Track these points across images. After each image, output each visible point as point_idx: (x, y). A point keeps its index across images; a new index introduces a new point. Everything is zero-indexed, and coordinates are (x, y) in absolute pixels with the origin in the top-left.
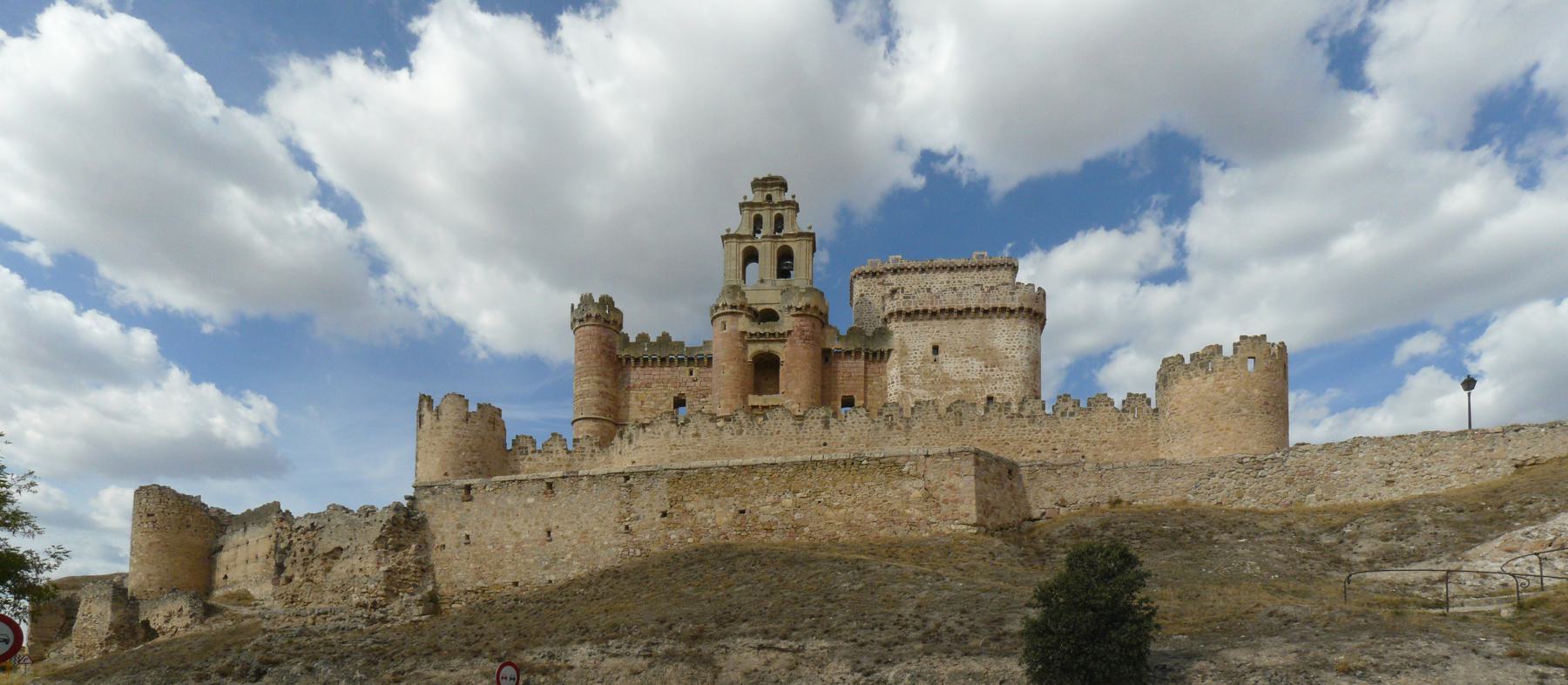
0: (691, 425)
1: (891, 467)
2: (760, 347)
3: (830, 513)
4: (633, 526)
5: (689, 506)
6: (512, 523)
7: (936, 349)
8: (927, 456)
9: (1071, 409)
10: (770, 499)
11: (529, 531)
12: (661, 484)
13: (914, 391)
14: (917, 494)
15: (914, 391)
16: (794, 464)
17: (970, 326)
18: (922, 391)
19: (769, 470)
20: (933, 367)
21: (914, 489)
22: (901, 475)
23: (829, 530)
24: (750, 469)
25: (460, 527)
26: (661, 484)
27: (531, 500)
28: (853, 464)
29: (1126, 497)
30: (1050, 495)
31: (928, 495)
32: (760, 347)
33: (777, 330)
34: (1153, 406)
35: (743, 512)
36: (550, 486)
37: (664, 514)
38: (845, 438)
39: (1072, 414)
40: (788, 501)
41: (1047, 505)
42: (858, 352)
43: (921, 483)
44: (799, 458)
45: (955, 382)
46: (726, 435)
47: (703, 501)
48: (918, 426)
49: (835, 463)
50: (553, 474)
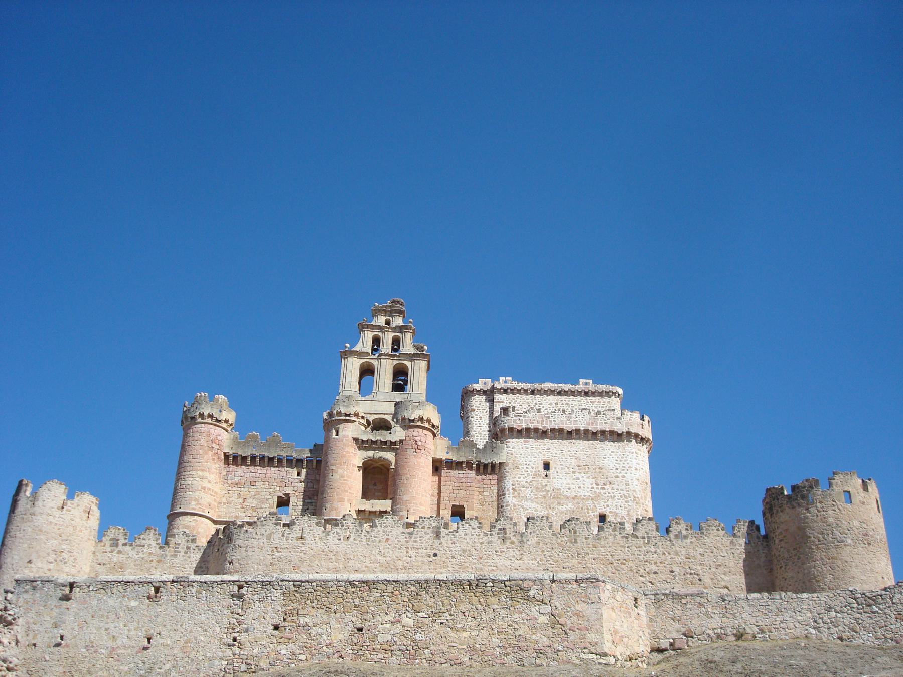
0: (296, 528)
1: (516, 590)
3: (452, 634)
4: (242, 638)
5: (303, 621)
6: (112, 626)
7: (547, 466)
8: (553, 581)
9: (684, 532)
10: (391, 617)
12: (277, 594)
13: (527, 504)
15: (527, 504)
16: (418, 582)
17: (581, 445)
18: (534, 505)
19: (390, 587)
20: (545, 482)
21: (540, 615)
22: (528, 599)
23: (454, 654)
24: (370, 584)
25: (56, 626)
26: (277, 594)
27: (134, 603)
29: (751, 630)
30: (677, 625)
31: (555, 621)
32: (371, 453)
34: (763, 532)
35: (360, 630)
36: (157, 590)
37: (276, 628)
39: (686, 537)
41: (675, 635)
43: (546, 609)
44: (420, 576)
45: (567, 498)
46: (332, 539)
47: (320, 615)
48: (533, 540)
49: (459, 583)
50: (164, 578)
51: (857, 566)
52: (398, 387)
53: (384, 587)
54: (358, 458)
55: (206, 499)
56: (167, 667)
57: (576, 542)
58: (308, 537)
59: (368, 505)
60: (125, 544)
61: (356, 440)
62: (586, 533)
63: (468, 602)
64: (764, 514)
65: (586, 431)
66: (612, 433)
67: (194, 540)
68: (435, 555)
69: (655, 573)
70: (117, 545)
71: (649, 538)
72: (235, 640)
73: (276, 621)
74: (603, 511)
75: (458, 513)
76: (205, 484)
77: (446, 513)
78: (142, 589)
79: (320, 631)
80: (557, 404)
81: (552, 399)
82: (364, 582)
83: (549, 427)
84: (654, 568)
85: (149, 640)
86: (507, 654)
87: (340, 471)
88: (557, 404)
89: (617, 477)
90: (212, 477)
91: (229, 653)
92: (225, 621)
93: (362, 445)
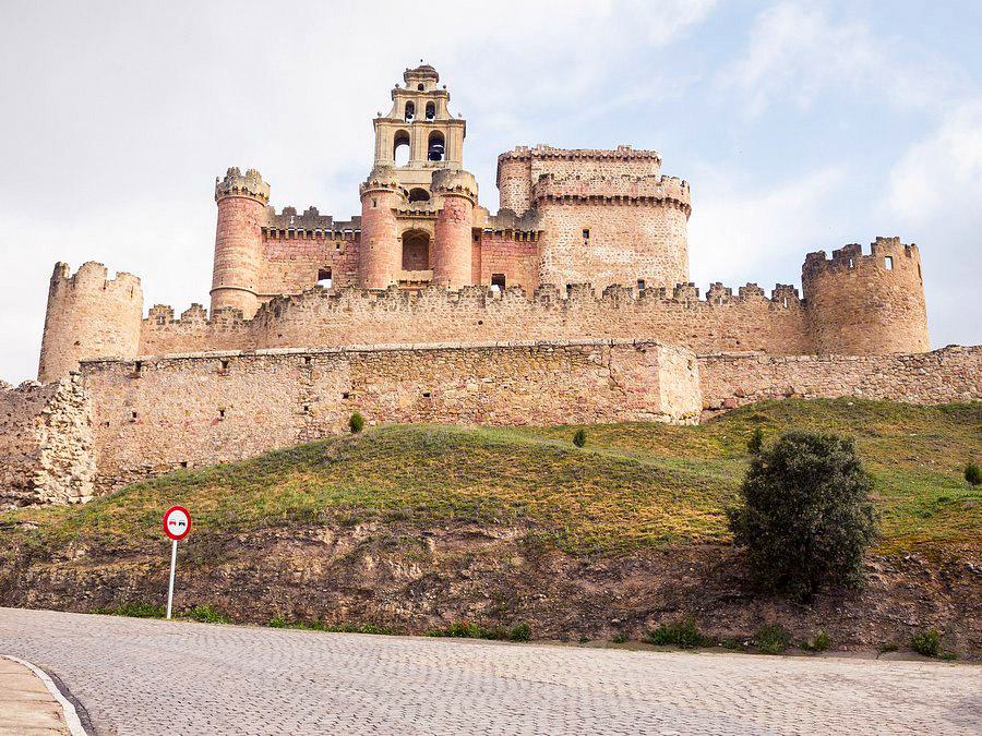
1: (576, 354)
2: (409, 224)
4: (313, 406)
5: (371, 388)
7: (586, 233)
9: (724, 297)
11: (200, 408)
13: (566, 272)
14: (602, 382)
15: (566, 272)
16: (480, 349)
19: (454, 355)
20: (584, 249)
23: (518, 415)
27: (203, 379)
28: (538, 350)
30: (728, 386)
31: (614, 384)
32: (409, 224)
33: (427, 209)
34: (801, 297)
35: (427, 395)
36: (225, 364)
38: (501, 317)
39: (725, 302)
40: (473, 386)
41: (726, 395)
42: (508, 232)
46: (379, 311)
47: (387, 384)
48: (576, 307)
50: (231, 353)
51: (894, 330)
52: (435, 156)
53: (448, 355)
54: (397, 229)
55: (248, 274)
56: (243, 436)
57: (618, 307)
58: (356, 309)
59: (409, 276)
60: (172, 322)
61: (394, 210)
62: (628, 299)
63: (534, 367)
64: (803, 279)
65: (626, 198)
66: (651, 199)
67: (240, 315)
68: (481, 323)
70: (164, 323)
71: (689, 303)
72: (306, 408)
73: (345, 390)
74: (641, 277)
75: (499, 280)
76: (245, 259)
77: (487, 281)
78: (211, 366)
79: (388, 398)
80: (595, 170)
81: (590, 165)
82: (428, 350)
83: (589, 194)
84: (693, 332)
85: (222, 412)
86: (569, 414)
87: (380, 243)
88: (595, 170)
89: (656, 244)
90: (252, 253)
91: (302, 422)
92: (295, 391)
93: (401, 216)
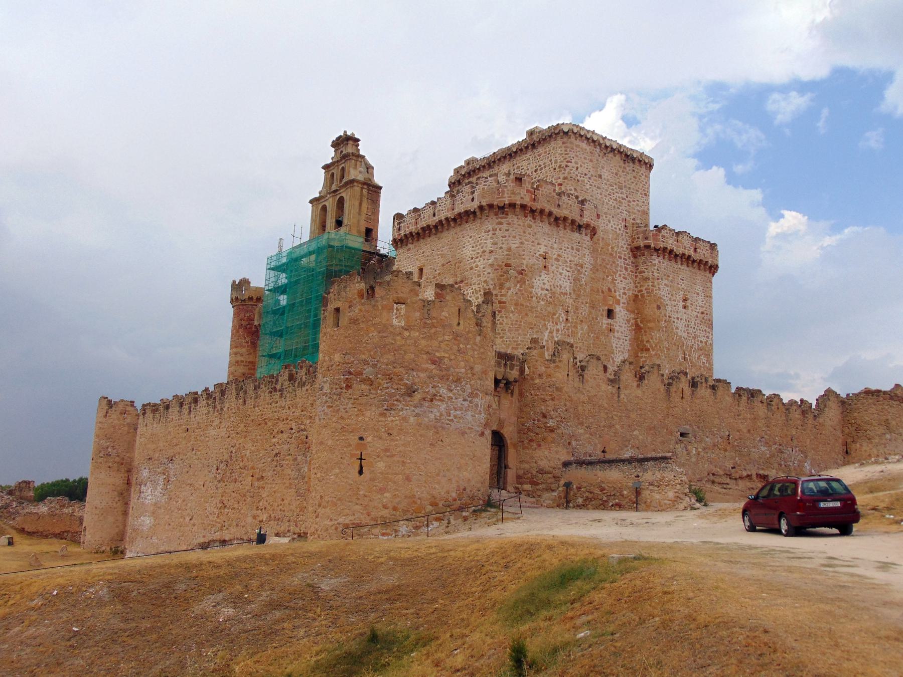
69: (282, 432)
